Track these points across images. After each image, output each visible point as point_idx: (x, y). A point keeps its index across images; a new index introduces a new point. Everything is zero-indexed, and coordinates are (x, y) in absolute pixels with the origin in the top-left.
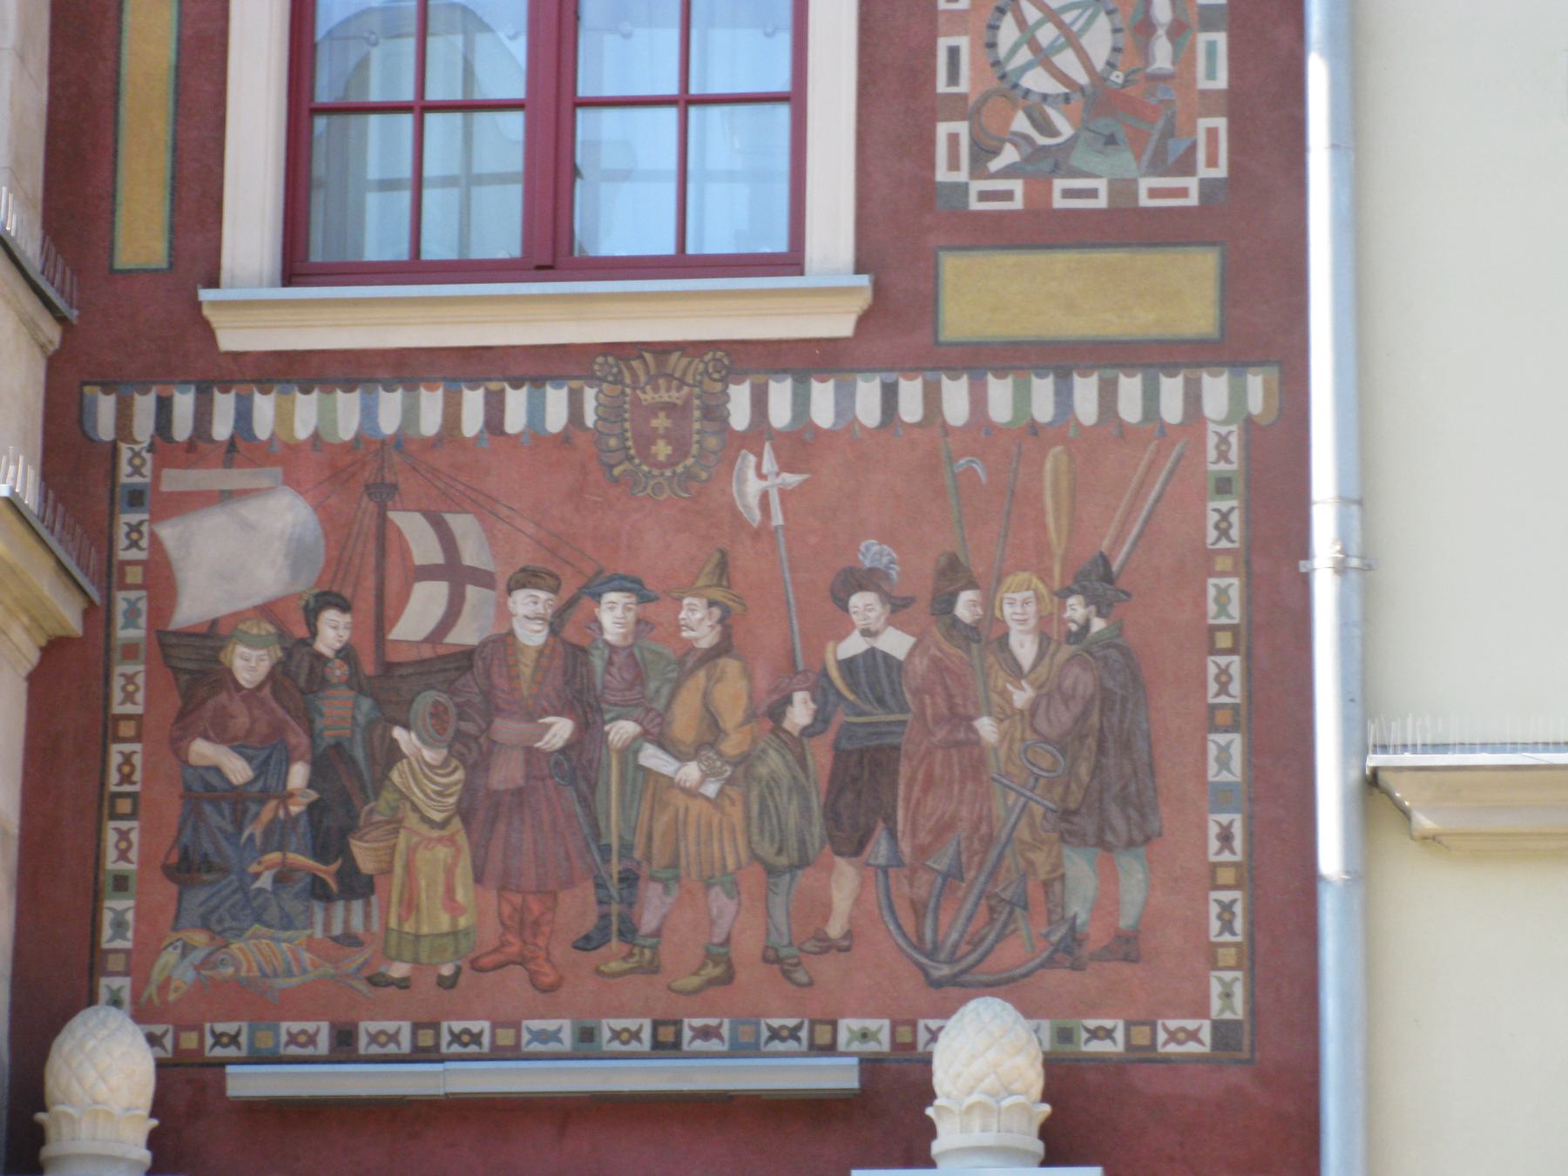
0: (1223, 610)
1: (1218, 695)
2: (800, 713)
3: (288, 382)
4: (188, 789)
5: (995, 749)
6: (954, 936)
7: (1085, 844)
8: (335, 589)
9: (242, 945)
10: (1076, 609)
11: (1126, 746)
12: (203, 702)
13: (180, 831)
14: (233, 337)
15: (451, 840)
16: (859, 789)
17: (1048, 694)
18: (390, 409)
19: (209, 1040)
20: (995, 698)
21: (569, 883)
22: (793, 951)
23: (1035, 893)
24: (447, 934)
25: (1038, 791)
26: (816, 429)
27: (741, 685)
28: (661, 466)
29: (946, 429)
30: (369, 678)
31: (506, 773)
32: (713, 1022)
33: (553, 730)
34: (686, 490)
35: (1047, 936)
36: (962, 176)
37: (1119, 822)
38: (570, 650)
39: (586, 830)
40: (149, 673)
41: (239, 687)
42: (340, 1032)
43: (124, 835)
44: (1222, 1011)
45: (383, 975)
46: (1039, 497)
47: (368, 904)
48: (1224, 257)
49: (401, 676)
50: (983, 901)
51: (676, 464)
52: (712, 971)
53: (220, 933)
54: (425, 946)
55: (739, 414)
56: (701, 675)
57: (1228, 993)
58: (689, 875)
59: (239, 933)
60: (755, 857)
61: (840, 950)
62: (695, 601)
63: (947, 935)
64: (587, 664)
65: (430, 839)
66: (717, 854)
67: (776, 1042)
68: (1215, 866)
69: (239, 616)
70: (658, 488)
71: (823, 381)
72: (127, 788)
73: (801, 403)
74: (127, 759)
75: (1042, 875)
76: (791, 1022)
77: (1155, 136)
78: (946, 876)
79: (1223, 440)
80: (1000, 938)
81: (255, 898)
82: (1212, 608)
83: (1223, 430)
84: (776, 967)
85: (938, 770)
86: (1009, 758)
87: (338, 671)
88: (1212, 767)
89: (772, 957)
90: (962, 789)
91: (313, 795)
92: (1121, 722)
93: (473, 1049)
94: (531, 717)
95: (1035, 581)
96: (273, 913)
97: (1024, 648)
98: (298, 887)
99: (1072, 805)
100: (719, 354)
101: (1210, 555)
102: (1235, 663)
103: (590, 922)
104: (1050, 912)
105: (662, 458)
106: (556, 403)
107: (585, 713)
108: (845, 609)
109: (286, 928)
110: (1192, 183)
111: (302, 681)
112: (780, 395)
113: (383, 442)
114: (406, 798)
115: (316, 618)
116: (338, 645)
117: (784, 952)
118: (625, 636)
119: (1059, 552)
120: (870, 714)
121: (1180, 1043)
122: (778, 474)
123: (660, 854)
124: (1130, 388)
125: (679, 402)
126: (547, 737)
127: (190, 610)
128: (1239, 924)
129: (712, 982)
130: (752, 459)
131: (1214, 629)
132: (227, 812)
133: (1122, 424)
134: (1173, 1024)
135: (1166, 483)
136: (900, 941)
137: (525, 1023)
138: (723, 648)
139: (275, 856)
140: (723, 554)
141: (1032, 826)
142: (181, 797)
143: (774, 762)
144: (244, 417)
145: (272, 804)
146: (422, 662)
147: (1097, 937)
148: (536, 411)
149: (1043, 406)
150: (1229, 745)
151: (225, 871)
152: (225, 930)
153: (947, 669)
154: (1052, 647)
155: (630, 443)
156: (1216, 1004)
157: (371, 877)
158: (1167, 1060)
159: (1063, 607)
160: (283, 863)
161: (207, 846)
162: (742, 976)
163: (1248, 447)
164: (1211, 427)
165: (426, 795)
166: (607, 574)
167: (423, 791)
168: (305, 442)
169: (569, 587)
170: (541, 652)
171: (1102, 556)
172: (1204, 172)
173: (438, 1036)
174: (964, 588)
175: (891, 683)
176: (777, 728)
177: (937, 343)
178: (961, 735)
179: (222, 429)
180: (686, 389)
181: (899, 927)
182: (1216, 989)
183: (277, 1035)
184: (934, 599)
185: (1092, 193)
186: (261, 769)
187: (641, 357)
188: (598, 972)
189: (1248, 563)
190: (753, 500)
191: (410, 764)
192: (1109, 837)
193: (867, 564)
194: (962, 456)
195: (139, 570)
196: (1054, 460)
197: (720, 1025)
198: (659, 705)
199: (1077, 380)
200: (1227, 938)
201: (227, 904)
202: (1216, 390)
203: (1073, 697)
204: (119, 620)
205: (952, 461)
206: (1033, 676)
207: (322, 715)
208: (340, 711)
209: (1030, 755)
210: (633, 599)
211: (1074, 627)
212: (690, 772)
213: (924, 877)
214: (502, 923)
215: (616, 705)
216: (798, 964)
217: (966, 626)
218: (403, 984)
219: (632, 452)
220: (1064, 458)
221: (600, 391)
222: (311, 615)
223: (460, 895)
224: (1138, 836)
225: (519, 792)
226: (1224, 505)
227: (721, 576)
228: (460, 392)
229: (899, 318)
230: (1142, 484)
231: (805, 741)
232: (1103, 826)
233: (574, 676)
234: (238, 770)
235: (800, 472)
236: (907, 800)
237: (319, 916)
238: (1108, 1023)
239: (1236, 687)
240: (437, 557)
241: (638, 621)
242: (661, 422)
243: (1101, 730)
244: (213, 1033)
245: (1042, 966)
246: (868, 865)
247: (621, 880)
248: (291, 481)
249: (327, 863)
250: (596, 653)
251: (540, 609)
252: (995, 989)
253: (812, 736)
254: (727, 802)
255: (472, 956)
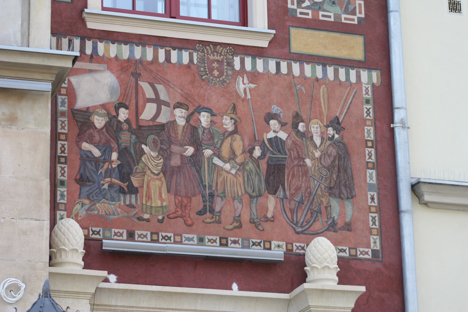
0: (369, 136)
1: (369, 159)
2: (257, 152)
3: (108, 40)
4: (82, 157)
5: (311, 168)
6: (302, 220)
7: (336, 197)
8: (124, 102)
9: (100, 205)
10: (331, 131)
11: (345, 171)
12: (86, 131)
13: (80, 169)
14: (91, 25)
15: (160, 179)
16: (275, 176)
17: (325, 154)
18: (138, 52)
19: (91, 233)
20: (310, 154)
21: (194, 195)
22: (258, 220)
23: (323, 210)
24: (160, 207)
25: (323, 181)
26: (259, 72)
27: (241, 143)
28: (216, 77)
29: (294, 77)
30: (134, 129)
31: (175, 161)
32: (237, 239)
33: (188, 150)
34: (223, 85)
35: (327, 222)
36: (295, 7)
37: (344, 192)
38: (192, 128)
39: (199, 180)
40: (68, 121)
41: (96, 128)
42: (130, 233)
43: (63, 169)
44: (374, 247)
45: (142, 217)
46: (319, 98)
47: (136, 196)
48: (364, 39)
49: (144, 130)
50: (309, 211)
51: (220, 77)
52: (236, 224)
53: (93, 201)
54: (154, 210)
55: (237, 66)
56: (230, 138)
57: (375, 242)
58: (228, 196)
59: (99, 201)
60: (246, 192)
61: (271, 221)
62: (227, 117)
63: (300, 219)
64: (197, 132)
65: (154, 179)
66: (236, 191)
67: (254, 246)
68: (370, 206)
69: (95, 107)
70: (215, 83)
71: (260, 59)
72: (63, 155)
73: (254, 64)
74: (63, 146)
75: (325, 205)
76: (259, 241)
77: (345, 4)
78: (299, 203)
79: (367, 89)
80: (314, 222)
81: (103, 191)
82: (366, 135)
83: (367, 86)
84: (254, 224)
85: (295, 172)
86: (315, 171)
87: (125, 126)
88: (368, 179)
89: (252, 221)
90: (302, 179)
91: (119, 162)
92: (344, 164)
93: (168, 241)
94: (182, 145)
95: (319, 122)
96: (108, 196)
97: (318, 141)
98: (116, 189)
99: (332, 186)
100: (231, 48)
101: (365, 120)
102: (373, 151)
103: (201, 207)
104: (327, 215)
105: (216, 75)
106: (185, 56)
107: (197, 146)
108: (269, 124)
109: (112, 201)
110: (355, 18)
111: (115, 128)
112: (248, 61)
113: (136, 61)
114: (147, 166)
115: (118, 111)
116: (125, 119)
117: (256, 220)
118: (208, 125)
119: (325, 114)
120: (275, 155)
121: (363, 255)
122: (248, 84)
123: (220, 190)
124: (342, 71)
125: (220, 60)
126: (186, 152)
127: (81, 104)
128: (377, 223)
129: (236, 227)
130: (241, 79)
131: (367, 141)
132: (94, 165)
133: (340, 81)
134: (361, 249)
135: (352, 99)
136: (287, 220)
137: (183, 235)
138: (235, 132)
139: (108, 179)
140: (234, 105)
141: (321, 191)
142: (80, 159)
143: (251, 166)
144: (95, 48)
145: (107, 164)
146: (150, 126)
147: (340, 224)
148: (180, 57)
149: (319, 74)
150: (372, 173)
151: (94, 182)
152: (94, 200)
153: (297, 144)
154: (325, 141)
155: (207, 70)
156: (372, 245)
157: (137, 188)
158: (360, 259)
159: (327, 130)
160: (111, 181)
161: (88, 174)
162: (244, 226)
163: (374, 92)
164: (364, 85)
165: (152, 165)
166: (202, 106)
167: (151, 164)
168: (113, 58)
169: (191, 109)
170: (184, 127)
171: (337, 117)
172: (358, 15)
173: (158, 236)
174: (300, 122)
175: (282, 146)
176: (251, 156)
177: (290, 52)
178: (302, 163)
179: (89, 51)
180: (222, 56)
181: (287, 216)
182: (372, 241)
183: (111, 233)
184: (292, 124)
185: (330, 17)
186: (104, 153)
187: (209, 46)
188: (203, 221)
189: (375, 123)
190: (242, 91)
191: (147, 156)
192: (342, 196)
193: (274, 112)
194: (299, 85)
195: (65, 90)
196: (323, 89)
197: (239, 240)
198: (218, 146)
199: (328, 67)
200: (374, 226)
201: (95, 192)
202: (364, 74)
203: (331, 155)
204: (59, 104)
205: (296, 86)
206: (320, 149)
207: (121, 139)
208: (126, 138)
209: (320, 170)
210: (210, 115)
211: (330, 136)
212: (227, 166)
213: (293, 203)
214: (176, 205)
215: (206, 145)
216: (260, 224)
217: (301, 132)
218: (148, 220)
219: (208, 72)
220: (326, 89)
221: (198, 54)
222: (117, 109)
223: (163, 196)
224: (350, 197)
225: (179, 167)
226: (368, 107)
227: (234, 110)
228: (158, 49)
229: (279, 46)
230: (346, 98)
231: (259, 161)
232: (340, 193)
233: (193, 135)
234: (97, 153)
235: (255, 84)
236: (288, 180)
237: (122, 198)
238: (344, 248)
239: (373, 157)
240: (153, 97)
241: (211, 121)
242: (215, 65)
243: (339, 165)
244: (92, 230)
245: (326, 230)
246: (277, 197)
247: (209, 195)
248: (109, 69)
249: (124, 183)
250: (200, 129)
251: (183, 114)
252: (322, 234)
253: (261, 159)
254: (238, 176)
255: (167, 214)
